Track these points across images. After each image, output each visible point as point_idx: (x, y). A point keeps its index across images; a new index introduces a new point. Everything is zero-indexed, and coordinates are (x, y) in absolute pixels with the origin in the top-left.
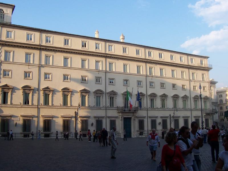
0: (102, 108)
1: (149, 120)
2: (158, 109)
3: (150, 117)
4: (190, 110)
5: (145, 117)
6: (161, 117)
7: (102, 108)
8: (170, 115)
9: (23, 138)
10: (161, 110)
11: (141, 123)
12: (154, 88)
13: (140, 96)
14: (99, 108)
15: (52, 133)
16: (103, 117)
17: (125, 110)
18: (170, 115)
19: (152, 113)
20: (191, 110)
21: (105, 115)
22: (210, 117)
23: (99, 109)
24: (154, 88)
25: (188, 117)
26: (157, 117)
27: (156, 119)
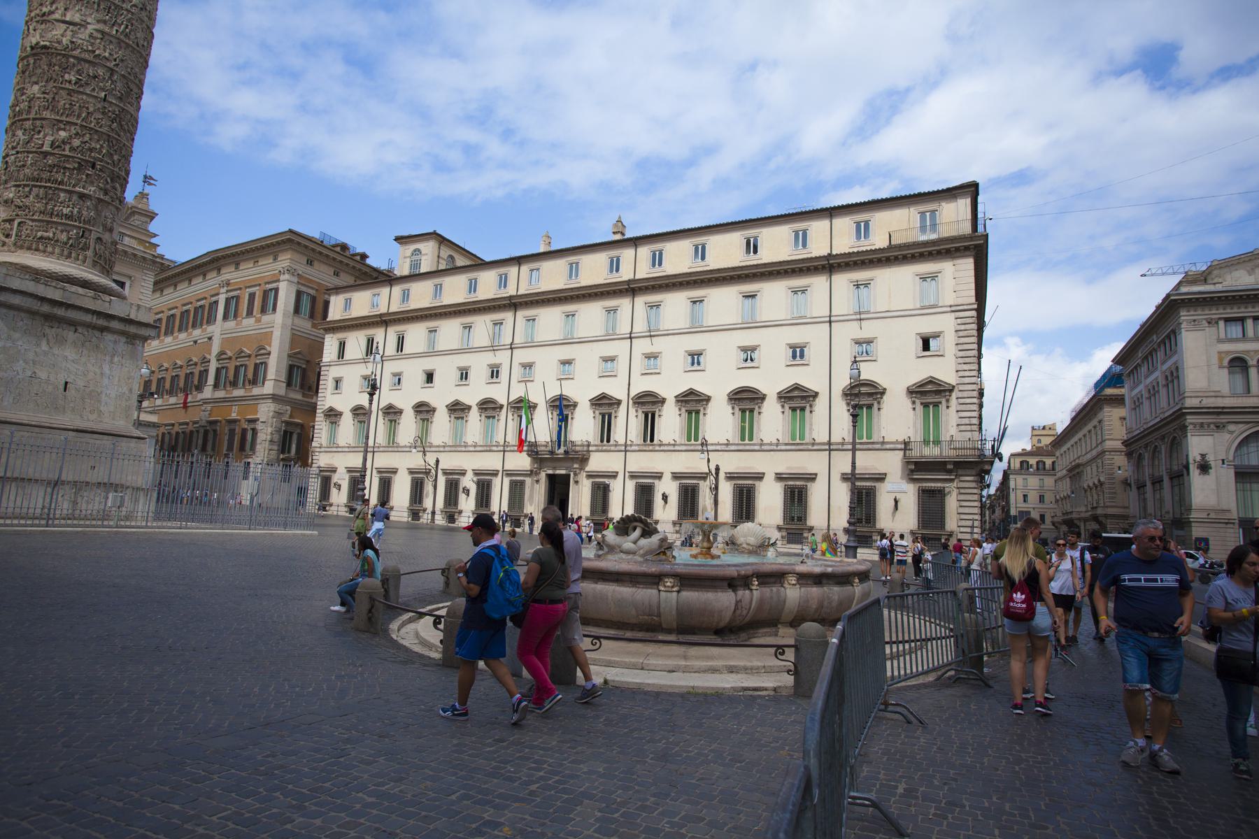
0: (495, 448)
1: (631, 486)
2: (672, 448)
3: (633, 476)
4: (827, 447)
5: (614, 476)
6: (676, 476)
7: (495, 448)
8: (717, 469)
9: (347, 515)
10: (684, 448)
11: (601, 494)
12: (942, 356)
13: (604, 405)
14: (488, 449)
15: (425, 510)
16: (495, 473)
17: (552, 452)
18: (717, 469)
19: (642, 462)
20: (830, 447)
21: (500, 469)
22: (952, 480)
23: (487, 451)
24: (942, 356)
25: (812, 478)
26: (659, 476)
27: (656, 482)
